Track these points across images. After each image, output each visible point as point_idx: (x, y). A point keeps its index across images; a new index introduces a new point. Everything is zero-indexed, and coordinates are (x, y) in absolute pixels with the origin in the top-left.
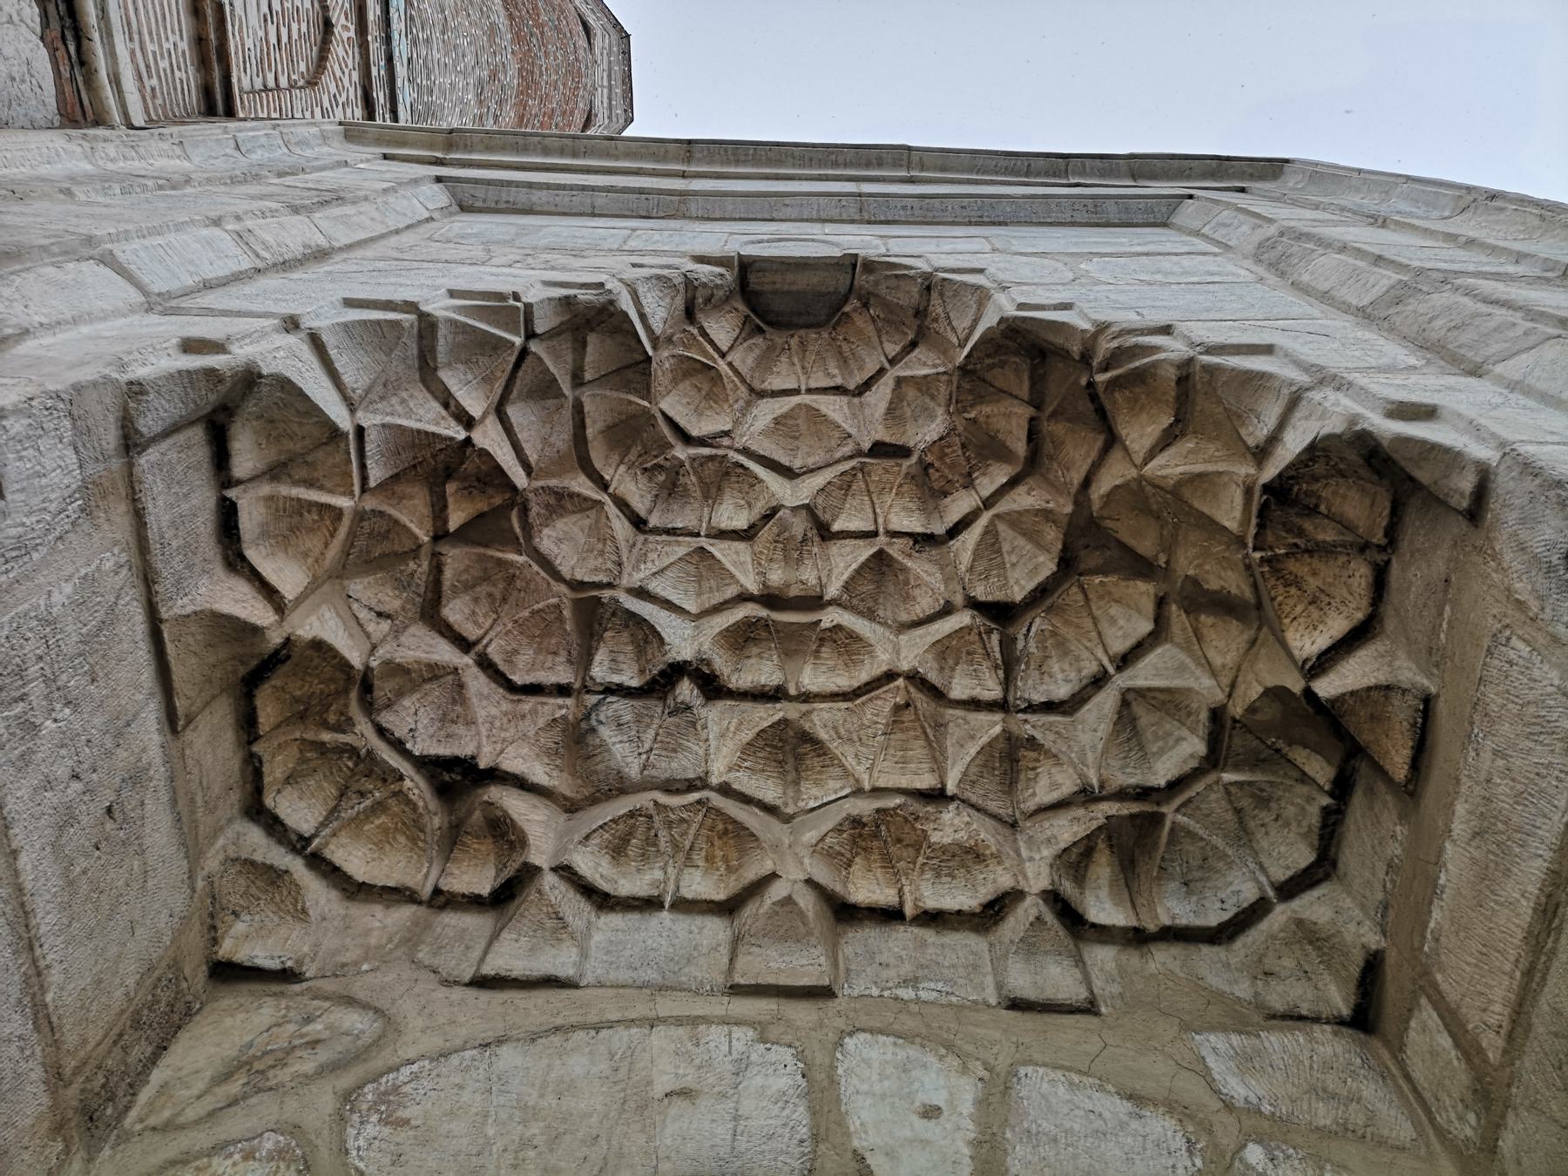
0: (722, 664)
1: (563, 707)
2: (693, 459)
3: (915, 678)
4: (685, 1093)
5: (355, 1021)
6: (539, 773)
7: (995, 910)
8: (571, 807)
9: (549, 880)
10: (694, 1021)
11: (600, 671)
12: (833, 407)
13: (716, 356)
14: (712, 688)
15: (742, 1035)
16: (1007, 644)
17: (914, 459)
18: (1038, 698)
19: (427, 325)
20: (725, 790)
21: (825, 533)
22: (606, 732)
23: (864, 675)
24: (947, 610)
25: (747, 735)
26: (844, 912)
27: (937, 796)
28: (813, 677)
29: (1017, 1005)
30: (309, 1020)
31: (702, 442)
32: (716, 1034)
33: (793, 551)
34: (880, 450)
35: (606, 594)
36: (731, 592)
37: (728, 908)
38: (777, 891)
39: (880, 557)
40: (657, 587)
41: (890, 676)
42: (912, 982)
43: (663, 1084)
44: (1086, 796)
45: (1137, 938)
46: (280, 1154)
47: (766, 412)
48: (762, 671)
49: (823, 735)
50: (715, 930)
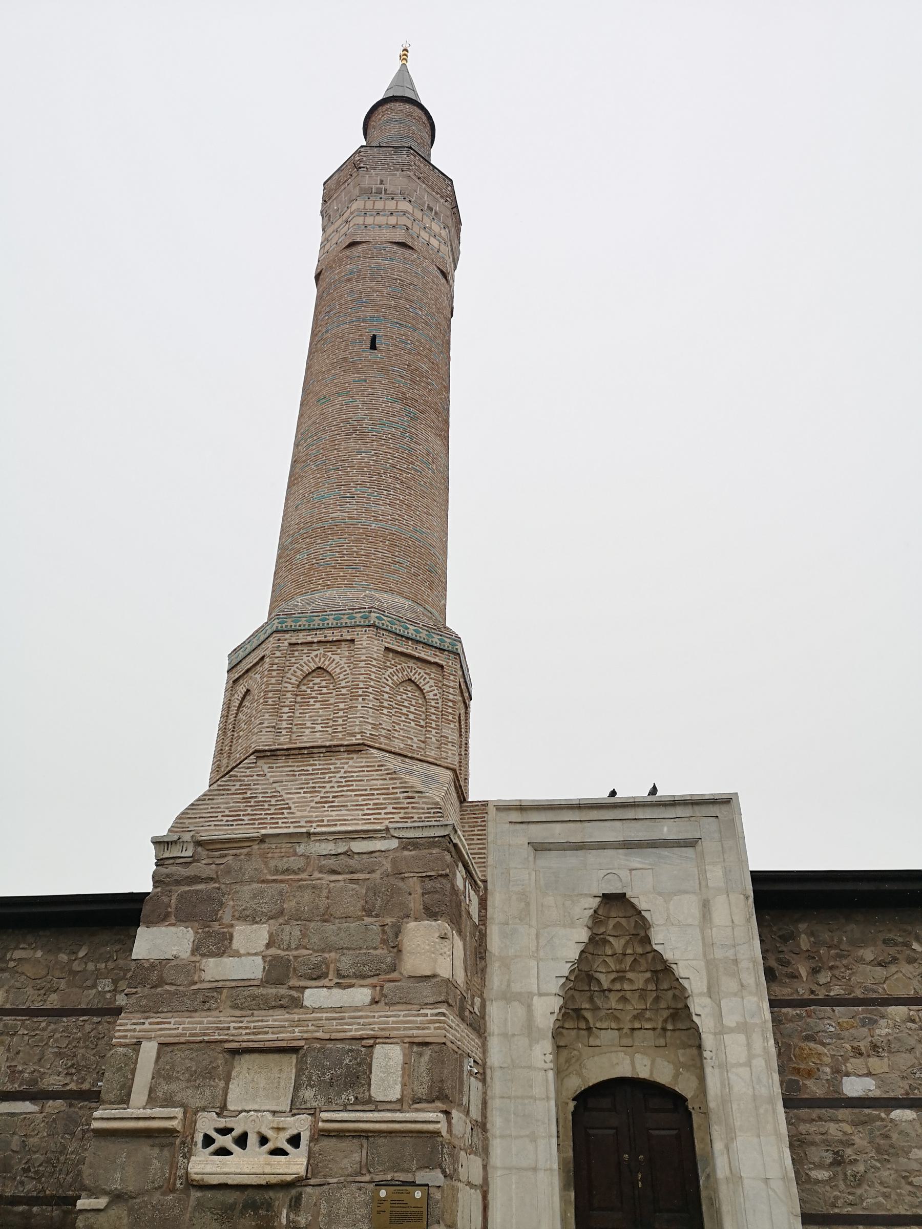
0: (611, 987)
1: (588, 994)
2: (600, 939)
3: (642, 990)
4: (617, 1064)
5: (576, 1052)
6: (587, 1006)
7: (654, 1029)
8: (592, 1010)
9: (594, 1029)
10: (617, 1051)
11: (592, 988)
12: (623, 921)
13: (600, 917)
14: (610, 990)
15: (623, 1053)
16: (658, 979)
17: (639, 937)
18: (662, 989)
19: (567, 978)
20: (615, 1009)
21: (625, 955)
22: (596, 999)
23: (634, 989)
24: (647, 971)
25: (617, 998)
26: (633, 1029)
27: (646, 1009)
28: (626, 986)
29: (656, 1047)
30: (571, 1053)
31: (601, 935)
32: (619, 1053)
33: (620, 962)
34: (633, 935)
35: (590, 973)
36: (610, 970)
37: (618, 1029)
38: (625, 1031)
39: (635, 959)
40: (599, 970)
41: (638, 989)
42: (643, 1042)
43: (614, 1063)
44: (668, 1008)
45: (674, 1030)
46: (576, 1074)
47: (612, 923)
48: (618, 986)
49: (628, 998)
50: (616, 1031)
